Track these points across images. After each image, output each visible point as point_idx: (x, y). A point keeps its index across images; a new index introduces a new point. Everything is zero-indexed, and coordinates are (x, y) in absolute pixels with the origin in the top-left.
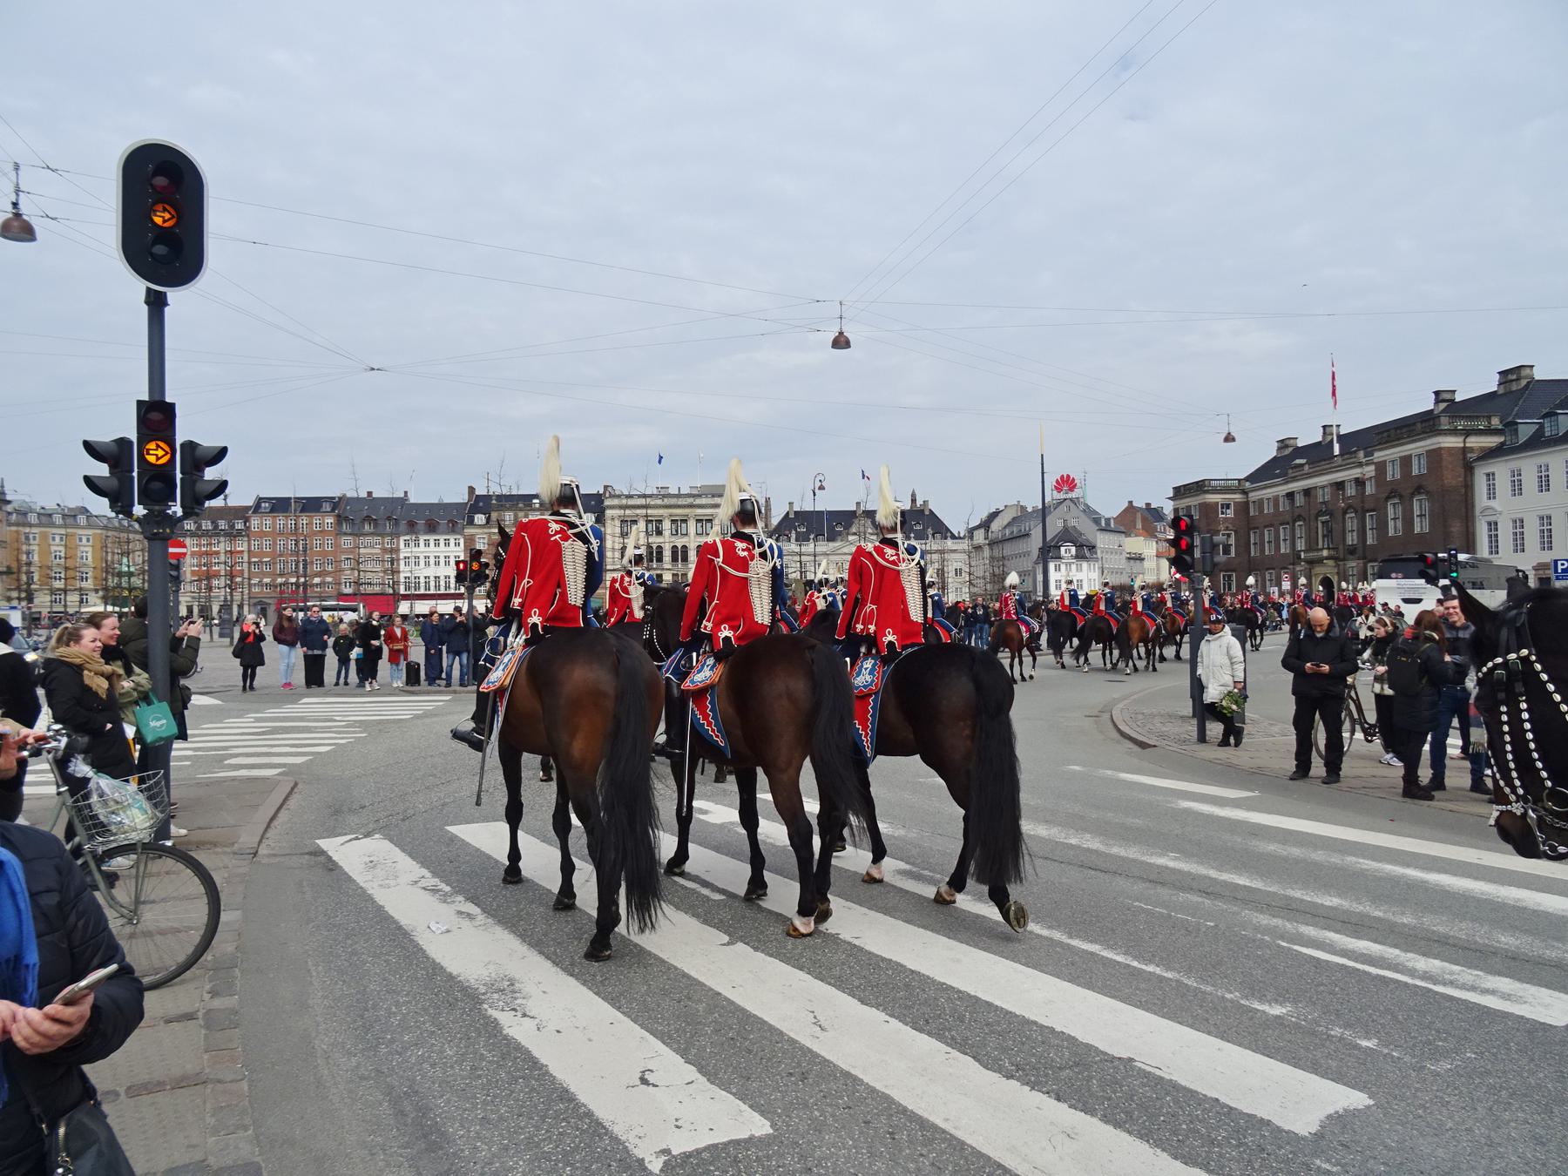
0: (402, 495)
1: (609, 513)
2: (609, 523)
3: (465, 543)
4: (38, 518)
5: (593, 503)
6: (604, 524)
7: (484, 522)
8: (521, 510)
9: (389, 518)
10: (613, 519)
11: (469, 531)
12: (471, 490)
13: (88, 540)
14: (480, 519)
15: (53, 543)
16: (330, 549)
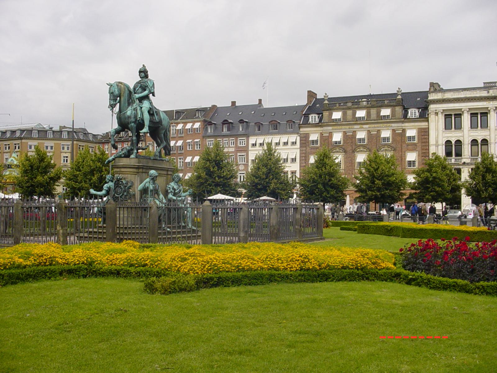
0: (257, 103)
1: (432, 107)
2: (432, 118)
3: (300, 140)
4: (38, 133)
5: (419, 99)
6: (428, 118)
7: (317, 120)
8: (349, 108)
9: (241, 121)
10: (437, 114)
11: (304, 130)
12: (311, 95)
13: (68, 149)
14: (313, 118)
15: (63, 151)
16: (198, 149)
